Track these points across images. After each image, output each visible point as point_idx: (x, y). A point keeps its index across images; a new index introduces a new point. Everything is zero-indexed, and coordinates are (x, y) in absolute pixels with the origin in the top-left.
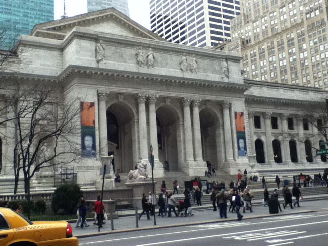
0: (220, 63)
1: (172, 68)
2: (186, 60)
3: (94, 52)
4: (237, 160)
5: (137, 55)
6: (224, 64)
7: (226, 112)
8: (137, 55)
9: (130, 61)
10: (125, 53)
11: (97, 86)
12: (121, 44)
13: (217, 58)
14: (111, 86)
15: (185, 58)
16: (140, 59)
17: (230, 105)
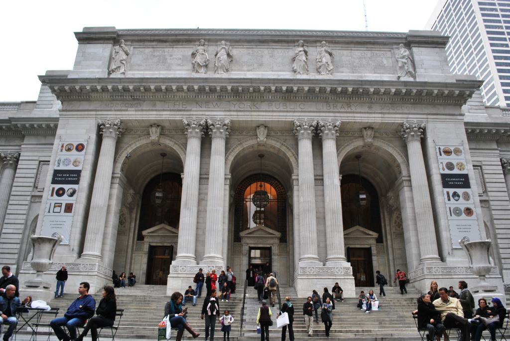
0: (393, 55)
1: (272, 71)
2: (306, 52)
3: (107, 59)
4: (449, 259)
5: (194, 55)
6: (403, 51)
7: (414, 148)
8: (194, 55)
9: (179, 68)
10: (171, 56)
11: (98, 113)
12: (165, 41)
13: (384, 44)
14: (127, 110)
15: (301, 49)
16: (198, 59)
17: (424, 131)
